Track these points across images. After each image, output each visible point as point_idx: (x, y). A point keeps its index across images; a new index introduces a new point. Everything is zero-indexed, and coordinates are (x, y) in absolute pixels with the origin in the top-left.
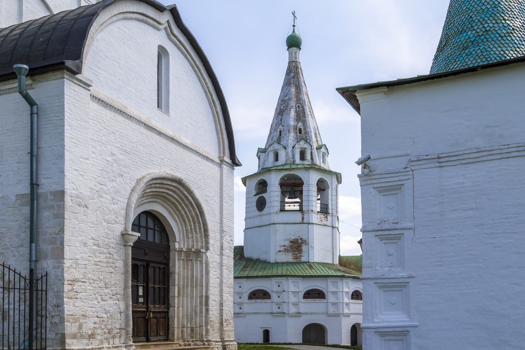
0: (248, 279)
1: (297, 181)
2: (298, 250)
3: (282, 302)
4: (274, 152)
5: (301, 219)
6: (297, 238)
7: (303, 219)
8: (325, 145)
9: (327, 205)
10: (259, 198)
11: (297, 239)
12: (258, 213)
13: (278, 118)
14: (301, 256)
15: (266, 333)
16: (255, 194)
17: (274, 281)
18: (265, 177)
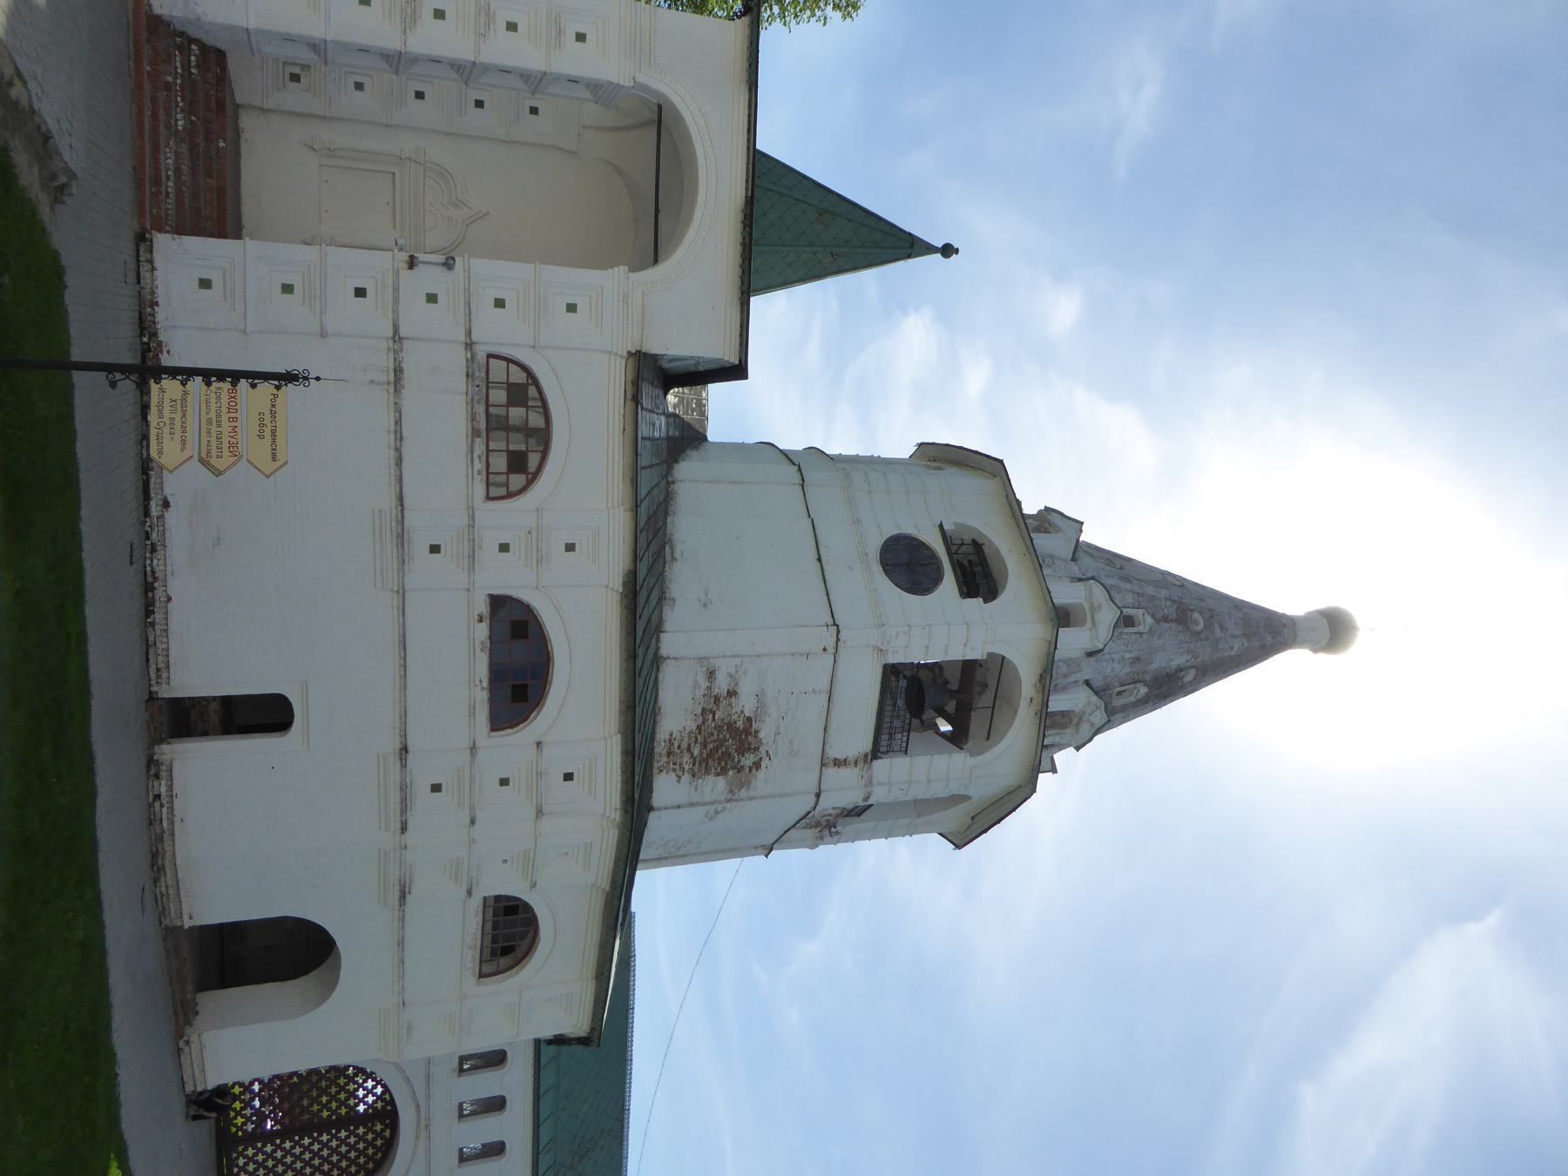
2: (710, 755)
3: (472, 809)
5: (840, 756)
6: (763, 750)
7: (837, 763)
11: (756, 749)
13: (1168, 603)
14: (679, 771)
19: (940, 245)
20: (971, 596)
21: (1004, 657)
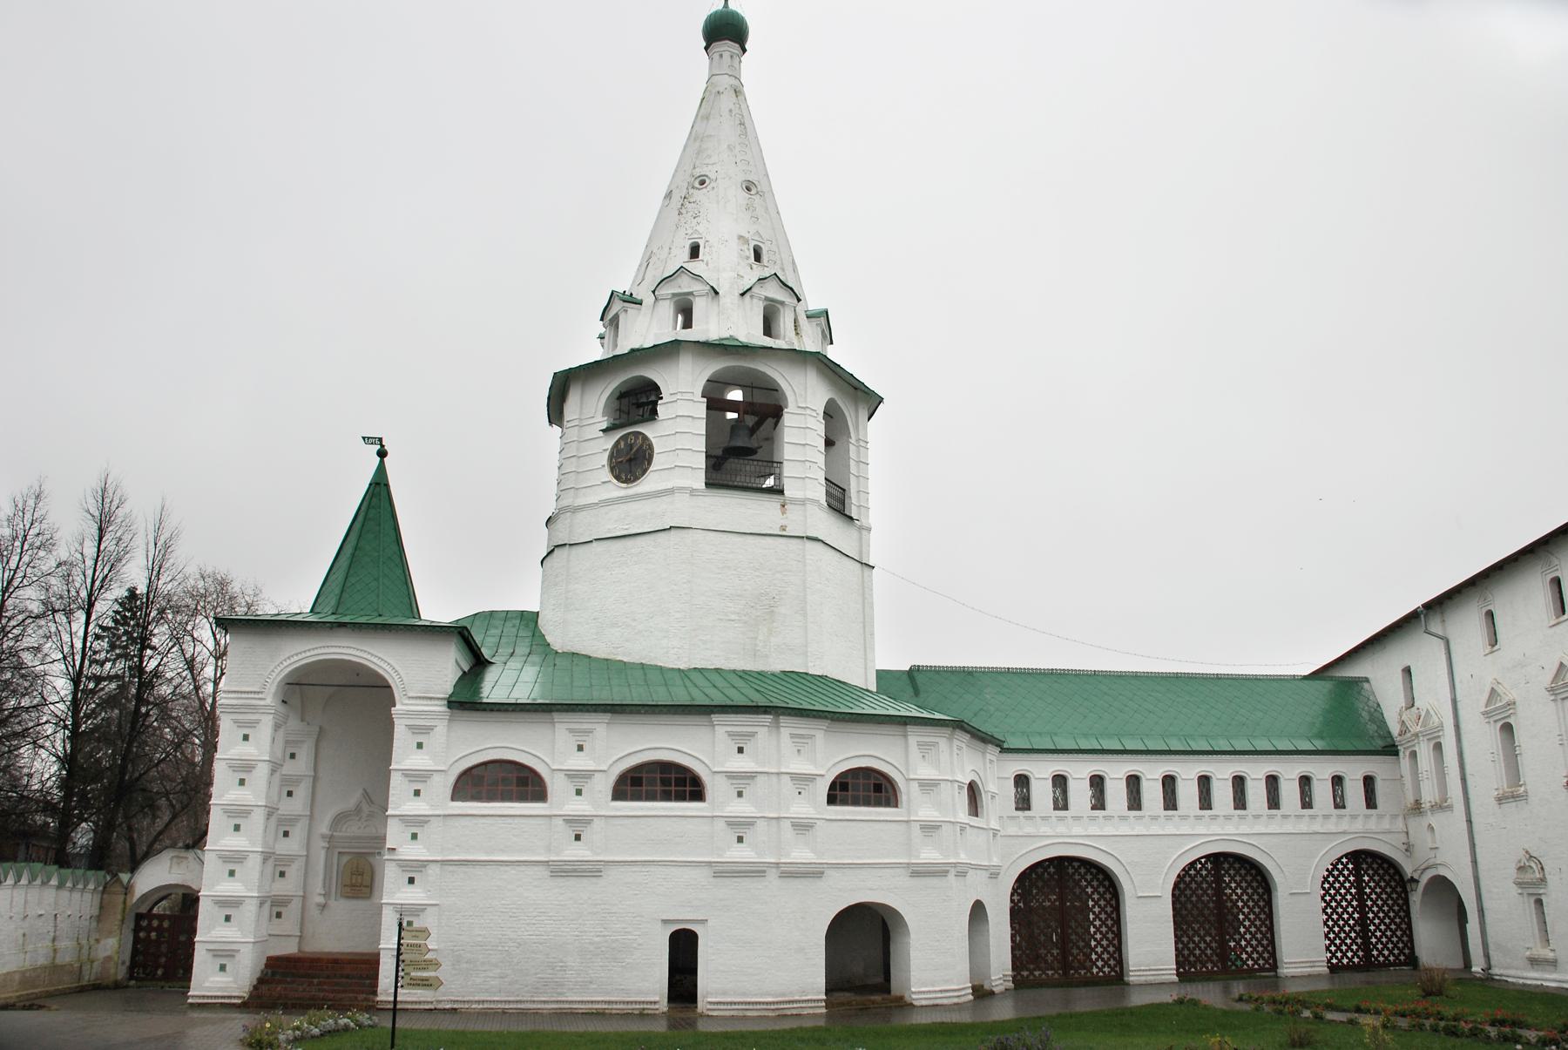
0: (615, 715)
1: (759, 398)
4: (675, 302)
8: (827, 312)
9: (844, 490)
10: (624, 438)
12: (617, 490)
15: (683, 947)
16: (604, 426)
17: (724, 726)
18: (655, 374)
19: (379, 459)
20: (654, 412)
21: (708, 381)
